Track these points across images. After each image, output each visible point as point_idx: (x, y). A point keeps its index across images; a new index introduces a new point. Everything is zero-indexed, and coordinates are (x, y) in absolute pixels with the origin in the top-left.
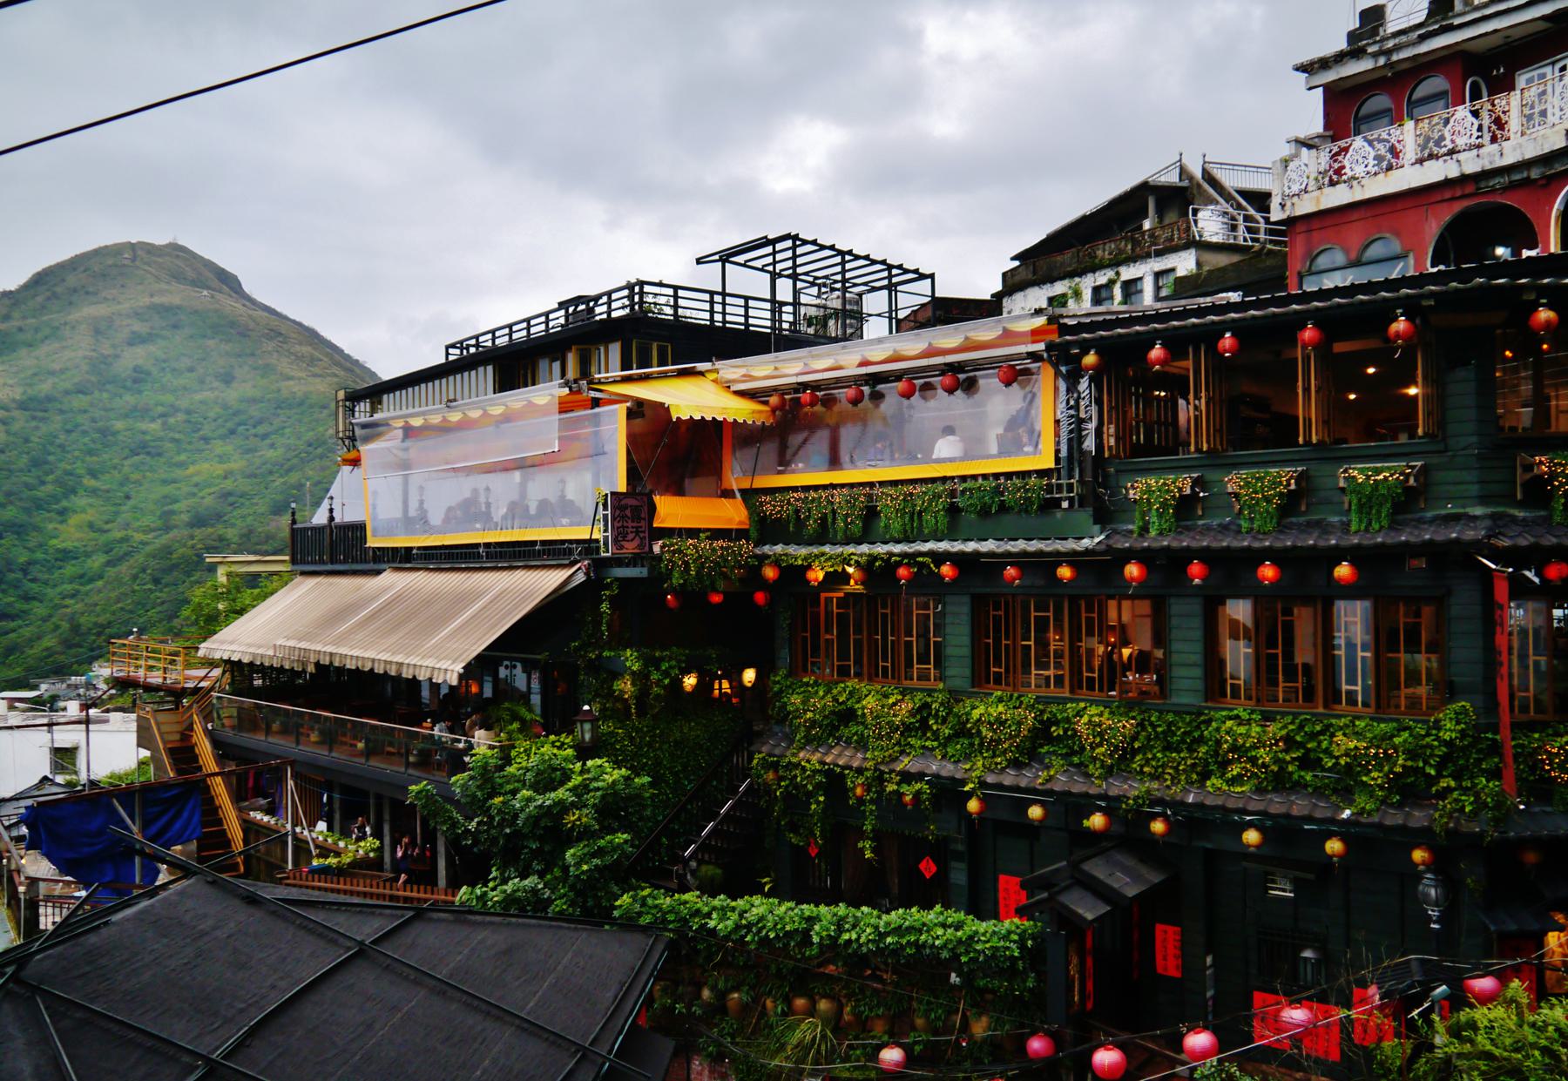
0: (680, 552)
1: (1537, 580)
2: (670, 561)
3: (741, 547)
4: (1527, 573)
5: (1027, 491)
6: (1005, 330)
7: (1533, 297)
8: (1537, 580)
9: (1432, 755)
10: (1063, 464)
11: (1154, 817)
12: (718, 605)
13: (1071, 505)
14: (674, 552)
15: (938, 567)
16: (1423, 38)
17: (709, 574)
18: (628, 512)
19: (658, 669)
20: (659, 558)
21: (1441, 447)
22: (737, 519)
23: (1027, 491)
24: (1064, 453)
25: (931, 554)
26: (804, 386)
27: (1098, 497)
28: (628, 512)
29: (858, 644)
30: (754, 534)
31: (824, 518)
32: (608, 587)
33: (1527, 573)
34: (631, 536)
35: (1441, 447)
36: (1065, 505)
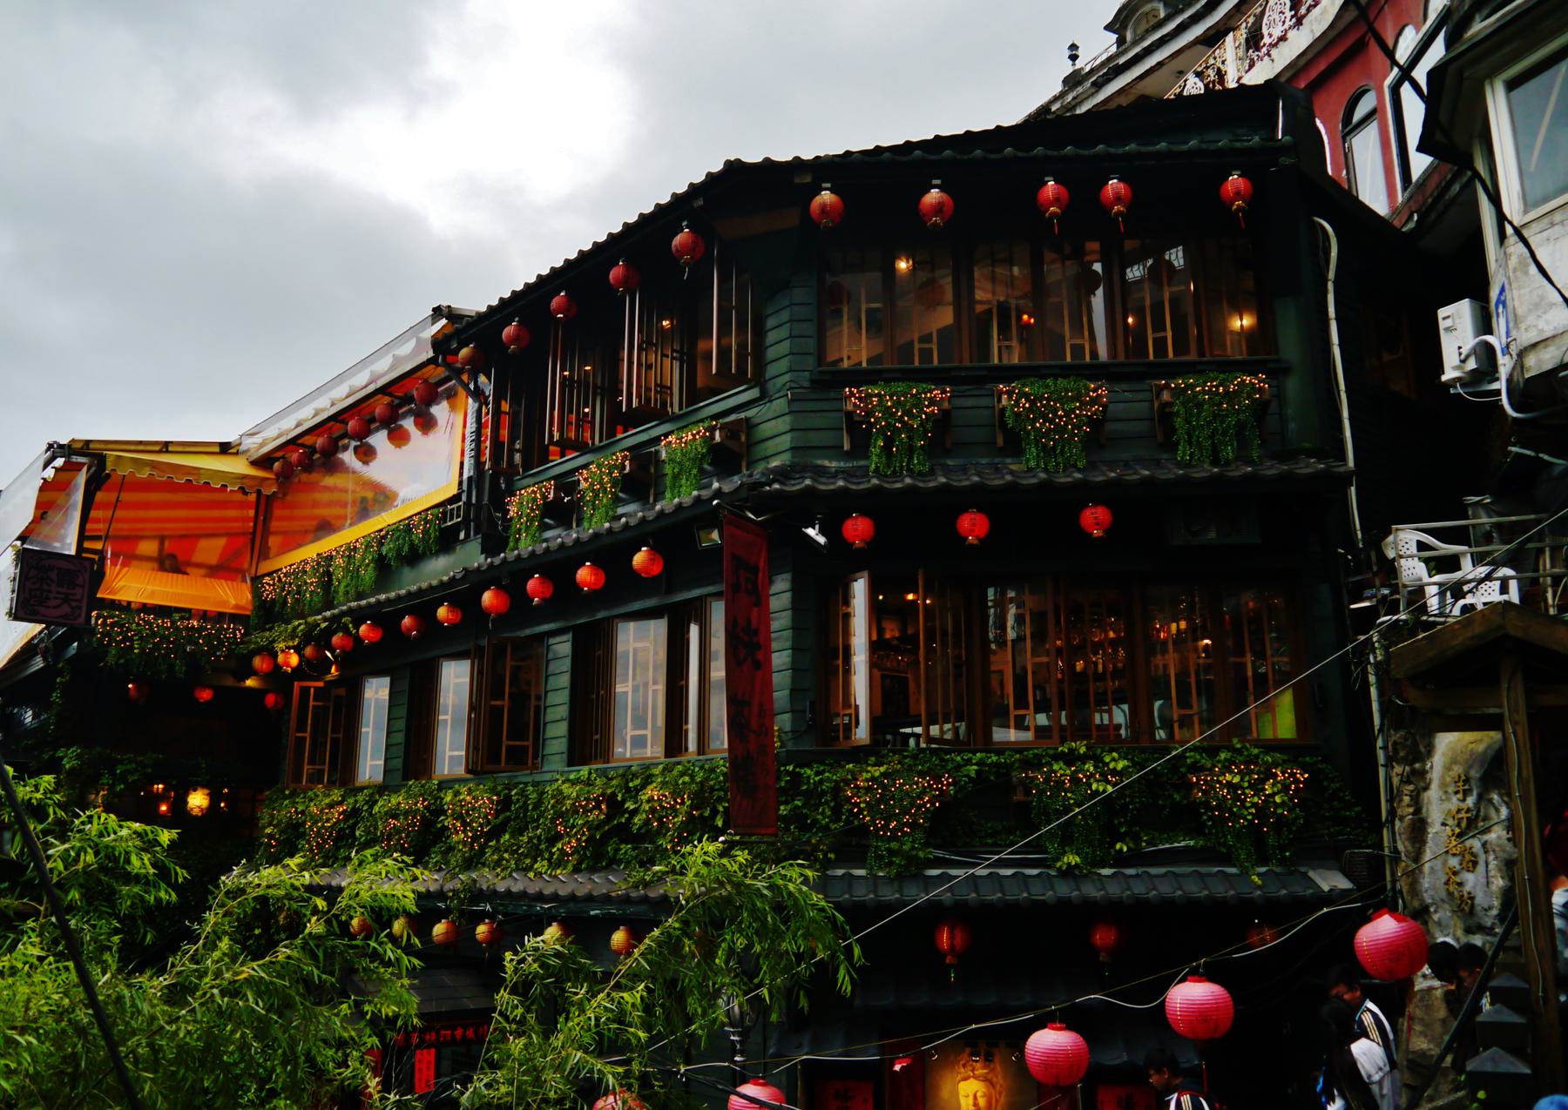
0: (122, 626)
1: (822, 540)
2: (108, 634)
3: (219, 631)
4: (811, 532)
5: (427, 521)
6: (419, 340)
7: (808, 179)
8: (822, 540)
9: (720, 800)
10: (465, 487)
11: (479, 918)
12: (207, 703)
13: (467, 536)
14: (113, 625)
15: (357, 627)
16: (1098, 86)
17: (167, 655)
18: (53, 575)
19: (112, 773)
20: (93, 632)
21: (754, 393)
22: (233, 602)
23: (427, 521)
24: (465, 476)
25: (350, 612)
26: (293, 443)
27: (492, 523)
28: (53, 575)
29: (335, 742)
30: (254, 621)
31: (298, 593)
32: (60, 673)
33: (811, 532)
34: (53, 603)
35: (754, 393)
36: (462, 535)
